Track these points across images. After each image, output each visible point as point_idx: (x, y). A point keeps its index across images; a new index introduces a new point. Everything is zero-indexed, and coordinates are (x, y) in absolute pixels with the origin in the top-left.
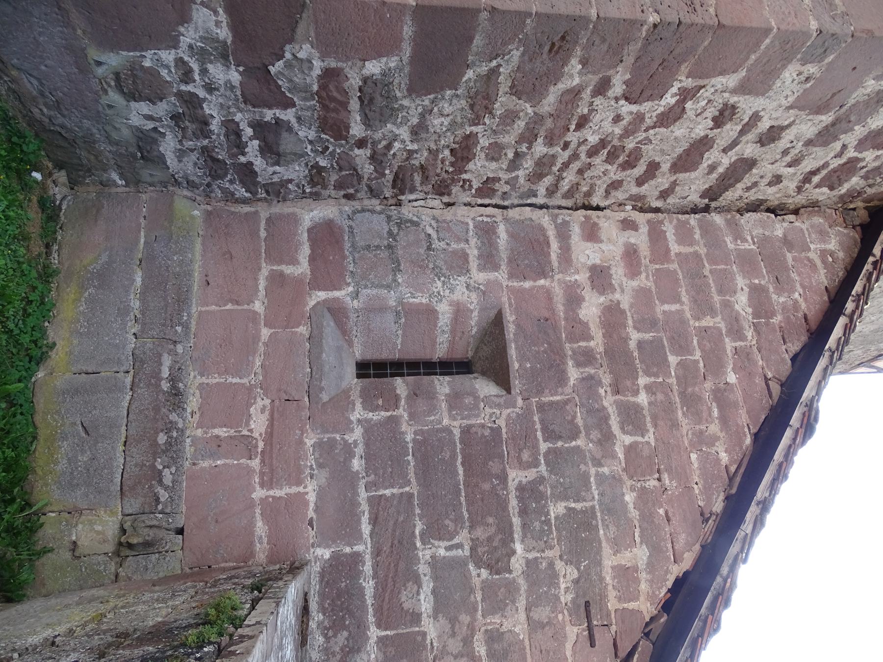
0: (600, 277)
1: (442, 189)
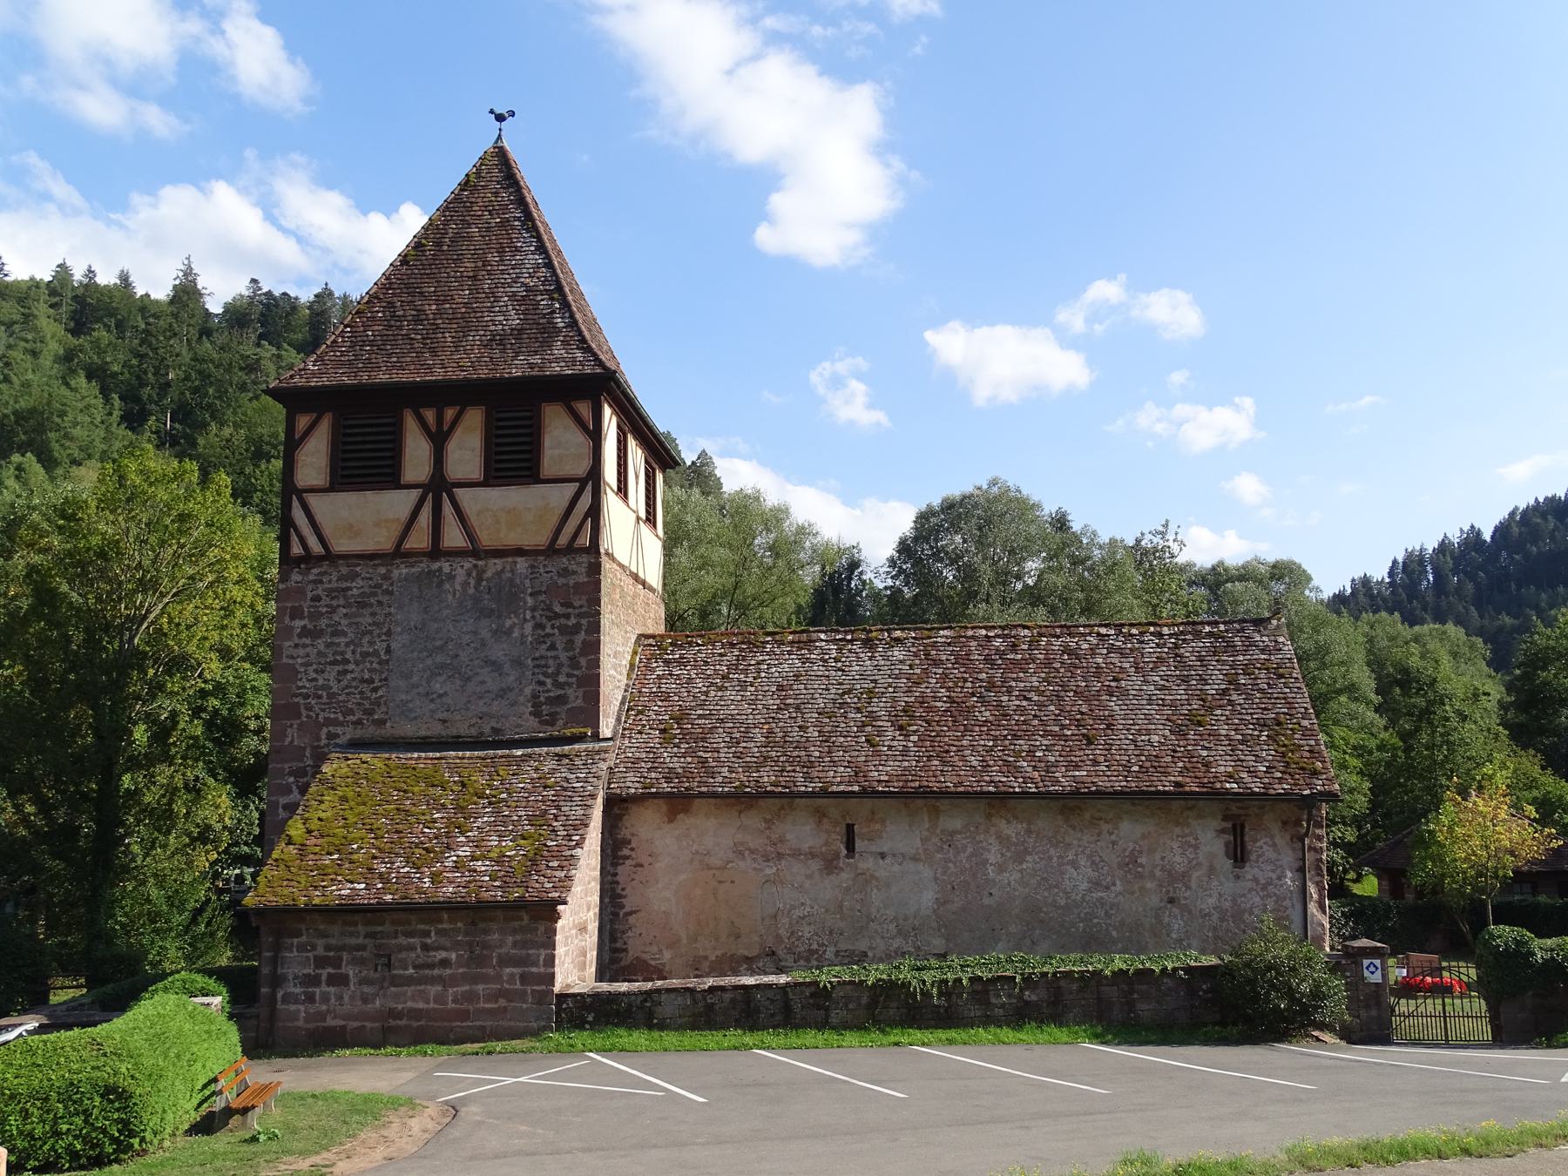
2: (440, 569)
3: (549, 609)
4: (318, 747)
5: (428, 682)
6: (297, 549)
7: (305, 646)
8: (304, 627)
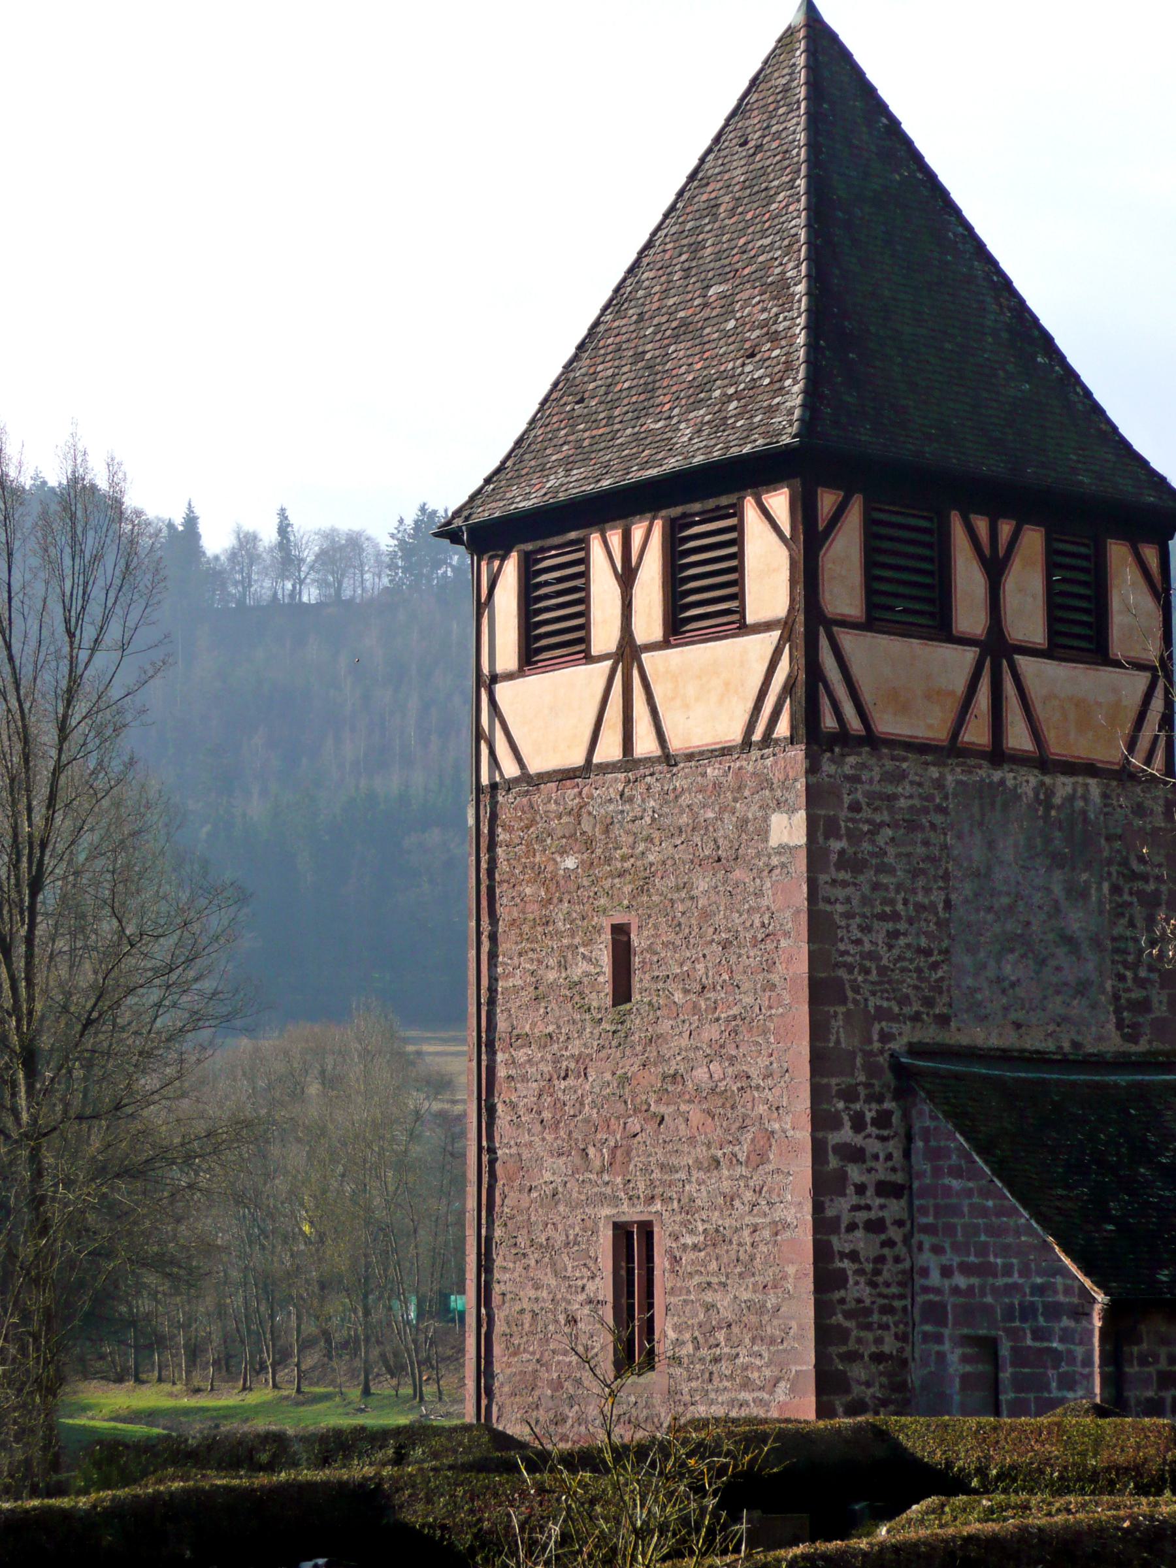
0: (946, 1272)
1: (904, 1363)
2: (1002, 782)
3: (1125, 863)
4: (870, 1054)
5: (998, 961)
6: (829, 722)
7: (845, 884)
8: (842, 852)
